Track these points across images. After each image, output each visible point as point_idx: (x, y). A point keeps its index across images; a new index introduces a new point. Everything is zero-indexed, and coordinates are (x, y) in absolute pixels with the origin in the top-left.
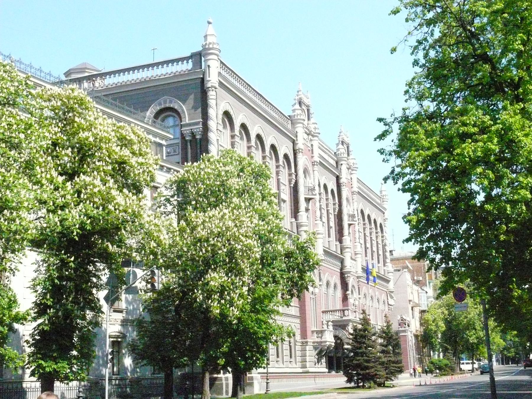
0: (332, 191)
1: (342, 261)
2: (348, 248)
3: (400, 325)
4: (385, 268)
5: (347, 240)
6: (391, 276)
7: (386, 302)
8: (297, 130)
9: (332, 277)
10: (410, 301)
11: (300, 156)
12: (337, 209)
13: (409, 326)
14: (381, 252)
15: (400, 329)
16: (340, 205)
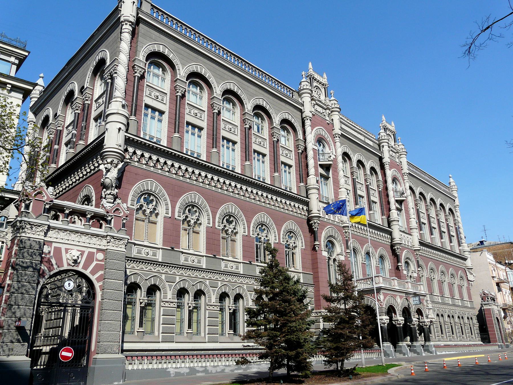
0: (372, 169)
1: (390, 233)
2: (395, 221)
3: (482, 299)
4: (461, 248)
5: (394, 214)
6: (467, 254)
7: (465, 278)
8: (303, 99)
9: (376, 248)
10: (493, 277)
11: (308, 123)
12: (381, 187)
13: (494, 301)
14: (453, 233)
15: (484, 303)
16: (385, 182)
